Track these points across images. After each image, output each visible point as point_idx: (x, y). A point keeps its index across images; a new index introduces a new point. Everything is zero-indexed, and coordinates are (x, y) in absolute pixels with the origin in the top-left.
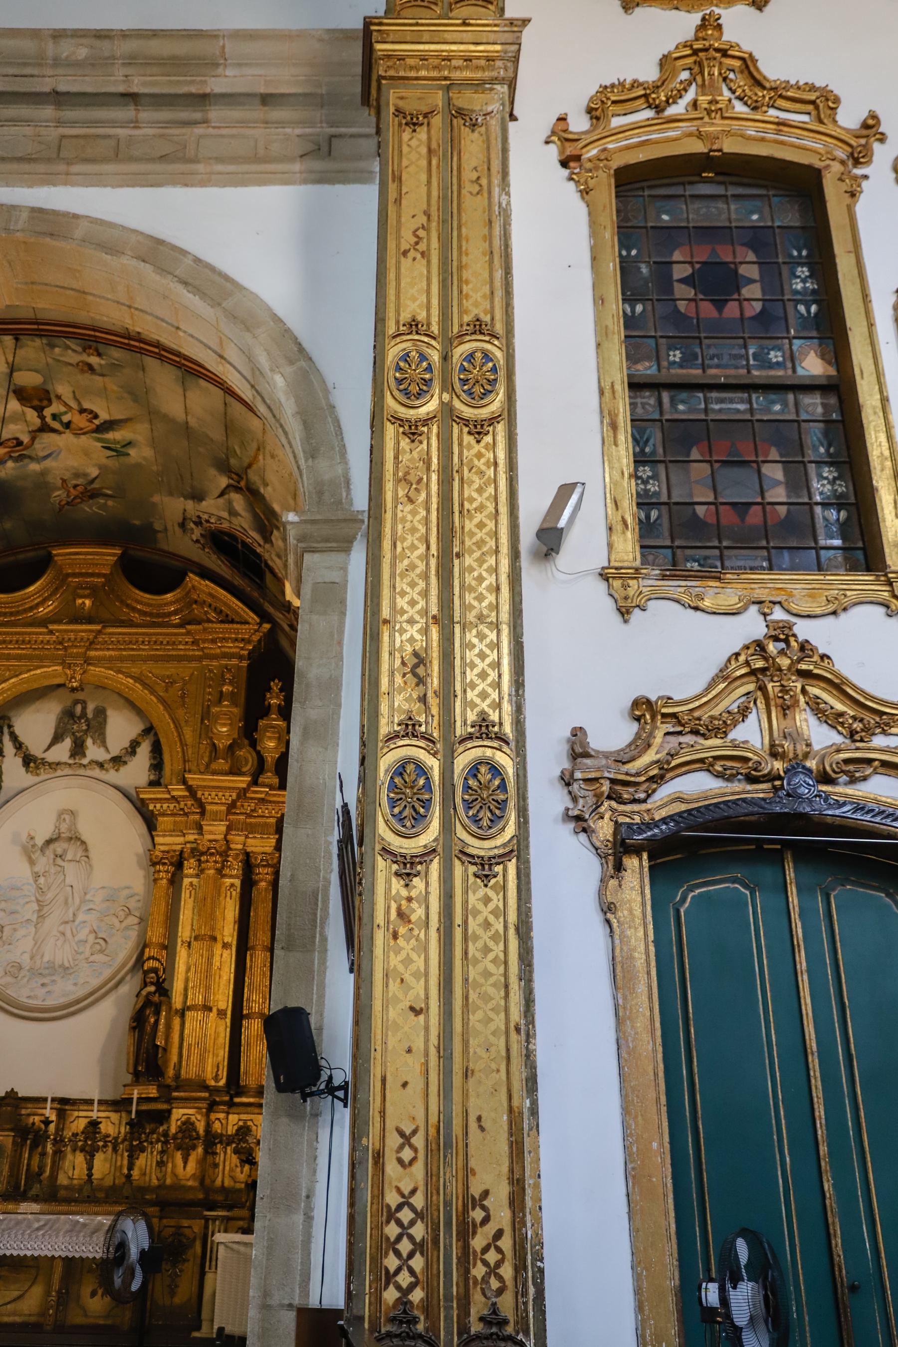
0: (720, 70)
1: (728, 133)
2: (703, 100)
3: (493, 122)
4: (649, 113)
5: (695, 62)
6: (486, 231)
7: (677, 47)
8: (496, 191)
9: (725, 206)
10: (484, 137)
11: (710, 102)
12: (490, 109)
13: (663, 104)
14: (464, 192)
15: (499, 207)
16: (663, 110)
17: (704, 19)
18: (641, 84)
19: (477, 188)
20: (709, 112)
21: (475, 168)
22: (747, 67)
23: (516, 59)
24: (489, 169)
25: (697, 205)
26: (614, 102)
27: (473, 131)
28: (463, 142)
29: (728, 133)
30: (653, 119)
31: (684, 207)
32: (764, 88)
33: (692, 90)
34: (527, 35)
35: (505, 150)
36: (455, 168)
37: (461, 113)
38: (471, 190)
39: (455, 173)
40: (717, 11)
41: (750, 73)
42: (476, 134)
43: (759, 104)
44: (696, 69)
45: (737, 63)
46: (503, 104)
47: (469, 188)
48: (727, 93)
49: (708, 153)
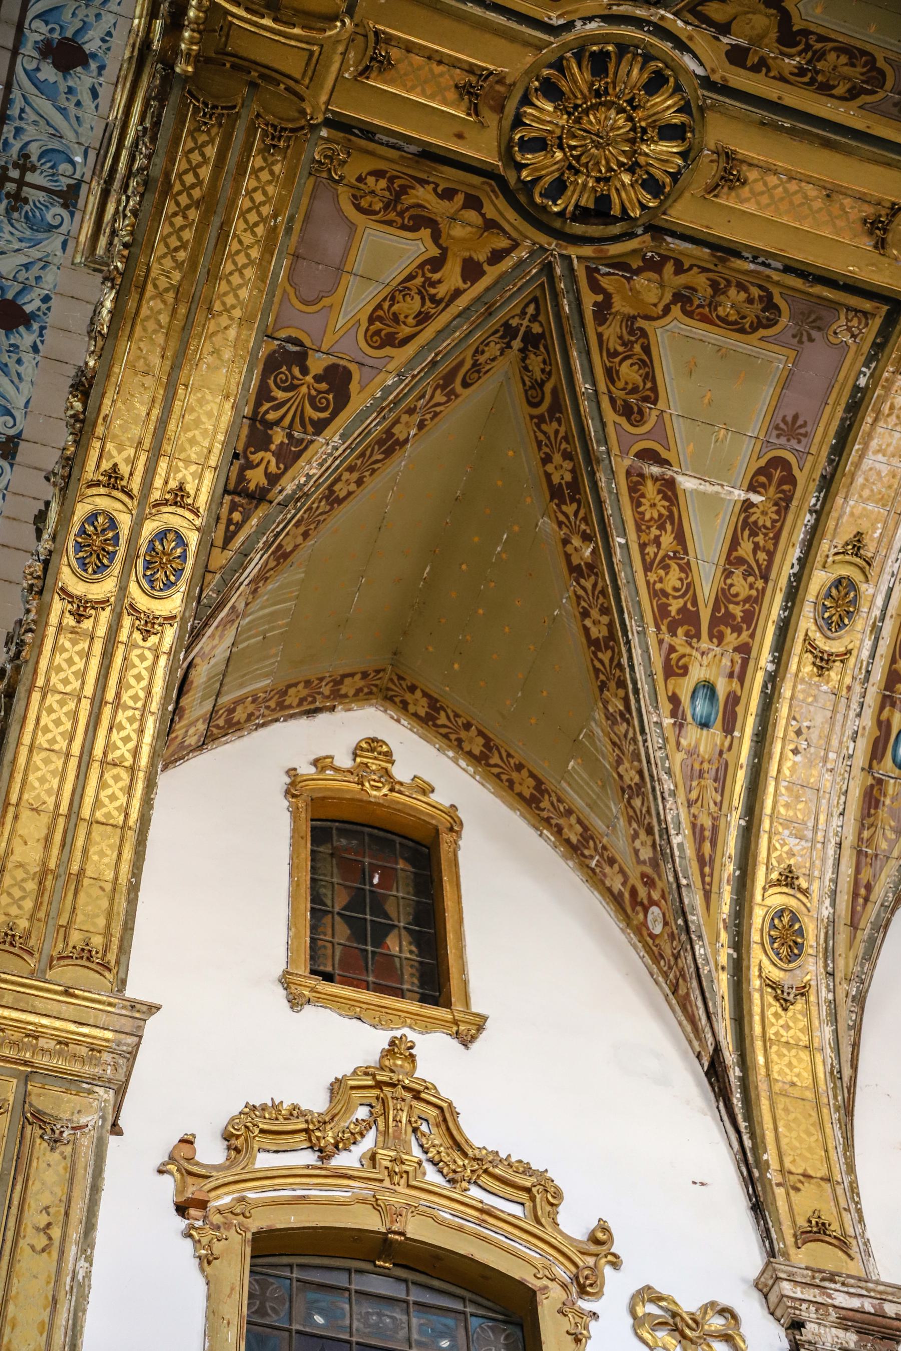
0: (409, 1116)
1: (415, 1210)
2: (385, 1155)
3: (85, 1141)
4: (309, 1158)
5: (377, 1098)
6: (45, 1315)
7: (355, 1072)
8: (72, 1250)
9: (404, 1318)
10: (69, 1159)
11: (393, 1160)
12: (83, 1121)
13: (330, 1148)
14: (22, 1243)
15: (73, 1279)
16: (329, 1157)
17: (392, 1043)
18: (302, 1114)
19: (44, 1241)
20: (391, 1174)
21: (46, 1208)
22: (445, 1120)
23: (132, 1055)
24: (67, 1214)
25: (367, 1307)
26: (262, 1131)
27: (53, 1149)
28: (34, 1164)
29: (415, 1210)
30: (315, 1168)
31: (347, 1307)
32: (465, 1155)
33: (371, 1135)
34: (152, 1026)
35: (96, 1189)
36: (16, 1202)
37: (39, 1118)
38: (34, 1242)
39: (14, 1210)
40: (412, 1035)
41: (448, 1129)
42: (56, 1155)
43: (457, 1177)
44: (378, 1108)
45: (433, 1112)
46: (103, 1118)
47: (32, 1238)
48: (417, 1152)
49: (386, 1234)
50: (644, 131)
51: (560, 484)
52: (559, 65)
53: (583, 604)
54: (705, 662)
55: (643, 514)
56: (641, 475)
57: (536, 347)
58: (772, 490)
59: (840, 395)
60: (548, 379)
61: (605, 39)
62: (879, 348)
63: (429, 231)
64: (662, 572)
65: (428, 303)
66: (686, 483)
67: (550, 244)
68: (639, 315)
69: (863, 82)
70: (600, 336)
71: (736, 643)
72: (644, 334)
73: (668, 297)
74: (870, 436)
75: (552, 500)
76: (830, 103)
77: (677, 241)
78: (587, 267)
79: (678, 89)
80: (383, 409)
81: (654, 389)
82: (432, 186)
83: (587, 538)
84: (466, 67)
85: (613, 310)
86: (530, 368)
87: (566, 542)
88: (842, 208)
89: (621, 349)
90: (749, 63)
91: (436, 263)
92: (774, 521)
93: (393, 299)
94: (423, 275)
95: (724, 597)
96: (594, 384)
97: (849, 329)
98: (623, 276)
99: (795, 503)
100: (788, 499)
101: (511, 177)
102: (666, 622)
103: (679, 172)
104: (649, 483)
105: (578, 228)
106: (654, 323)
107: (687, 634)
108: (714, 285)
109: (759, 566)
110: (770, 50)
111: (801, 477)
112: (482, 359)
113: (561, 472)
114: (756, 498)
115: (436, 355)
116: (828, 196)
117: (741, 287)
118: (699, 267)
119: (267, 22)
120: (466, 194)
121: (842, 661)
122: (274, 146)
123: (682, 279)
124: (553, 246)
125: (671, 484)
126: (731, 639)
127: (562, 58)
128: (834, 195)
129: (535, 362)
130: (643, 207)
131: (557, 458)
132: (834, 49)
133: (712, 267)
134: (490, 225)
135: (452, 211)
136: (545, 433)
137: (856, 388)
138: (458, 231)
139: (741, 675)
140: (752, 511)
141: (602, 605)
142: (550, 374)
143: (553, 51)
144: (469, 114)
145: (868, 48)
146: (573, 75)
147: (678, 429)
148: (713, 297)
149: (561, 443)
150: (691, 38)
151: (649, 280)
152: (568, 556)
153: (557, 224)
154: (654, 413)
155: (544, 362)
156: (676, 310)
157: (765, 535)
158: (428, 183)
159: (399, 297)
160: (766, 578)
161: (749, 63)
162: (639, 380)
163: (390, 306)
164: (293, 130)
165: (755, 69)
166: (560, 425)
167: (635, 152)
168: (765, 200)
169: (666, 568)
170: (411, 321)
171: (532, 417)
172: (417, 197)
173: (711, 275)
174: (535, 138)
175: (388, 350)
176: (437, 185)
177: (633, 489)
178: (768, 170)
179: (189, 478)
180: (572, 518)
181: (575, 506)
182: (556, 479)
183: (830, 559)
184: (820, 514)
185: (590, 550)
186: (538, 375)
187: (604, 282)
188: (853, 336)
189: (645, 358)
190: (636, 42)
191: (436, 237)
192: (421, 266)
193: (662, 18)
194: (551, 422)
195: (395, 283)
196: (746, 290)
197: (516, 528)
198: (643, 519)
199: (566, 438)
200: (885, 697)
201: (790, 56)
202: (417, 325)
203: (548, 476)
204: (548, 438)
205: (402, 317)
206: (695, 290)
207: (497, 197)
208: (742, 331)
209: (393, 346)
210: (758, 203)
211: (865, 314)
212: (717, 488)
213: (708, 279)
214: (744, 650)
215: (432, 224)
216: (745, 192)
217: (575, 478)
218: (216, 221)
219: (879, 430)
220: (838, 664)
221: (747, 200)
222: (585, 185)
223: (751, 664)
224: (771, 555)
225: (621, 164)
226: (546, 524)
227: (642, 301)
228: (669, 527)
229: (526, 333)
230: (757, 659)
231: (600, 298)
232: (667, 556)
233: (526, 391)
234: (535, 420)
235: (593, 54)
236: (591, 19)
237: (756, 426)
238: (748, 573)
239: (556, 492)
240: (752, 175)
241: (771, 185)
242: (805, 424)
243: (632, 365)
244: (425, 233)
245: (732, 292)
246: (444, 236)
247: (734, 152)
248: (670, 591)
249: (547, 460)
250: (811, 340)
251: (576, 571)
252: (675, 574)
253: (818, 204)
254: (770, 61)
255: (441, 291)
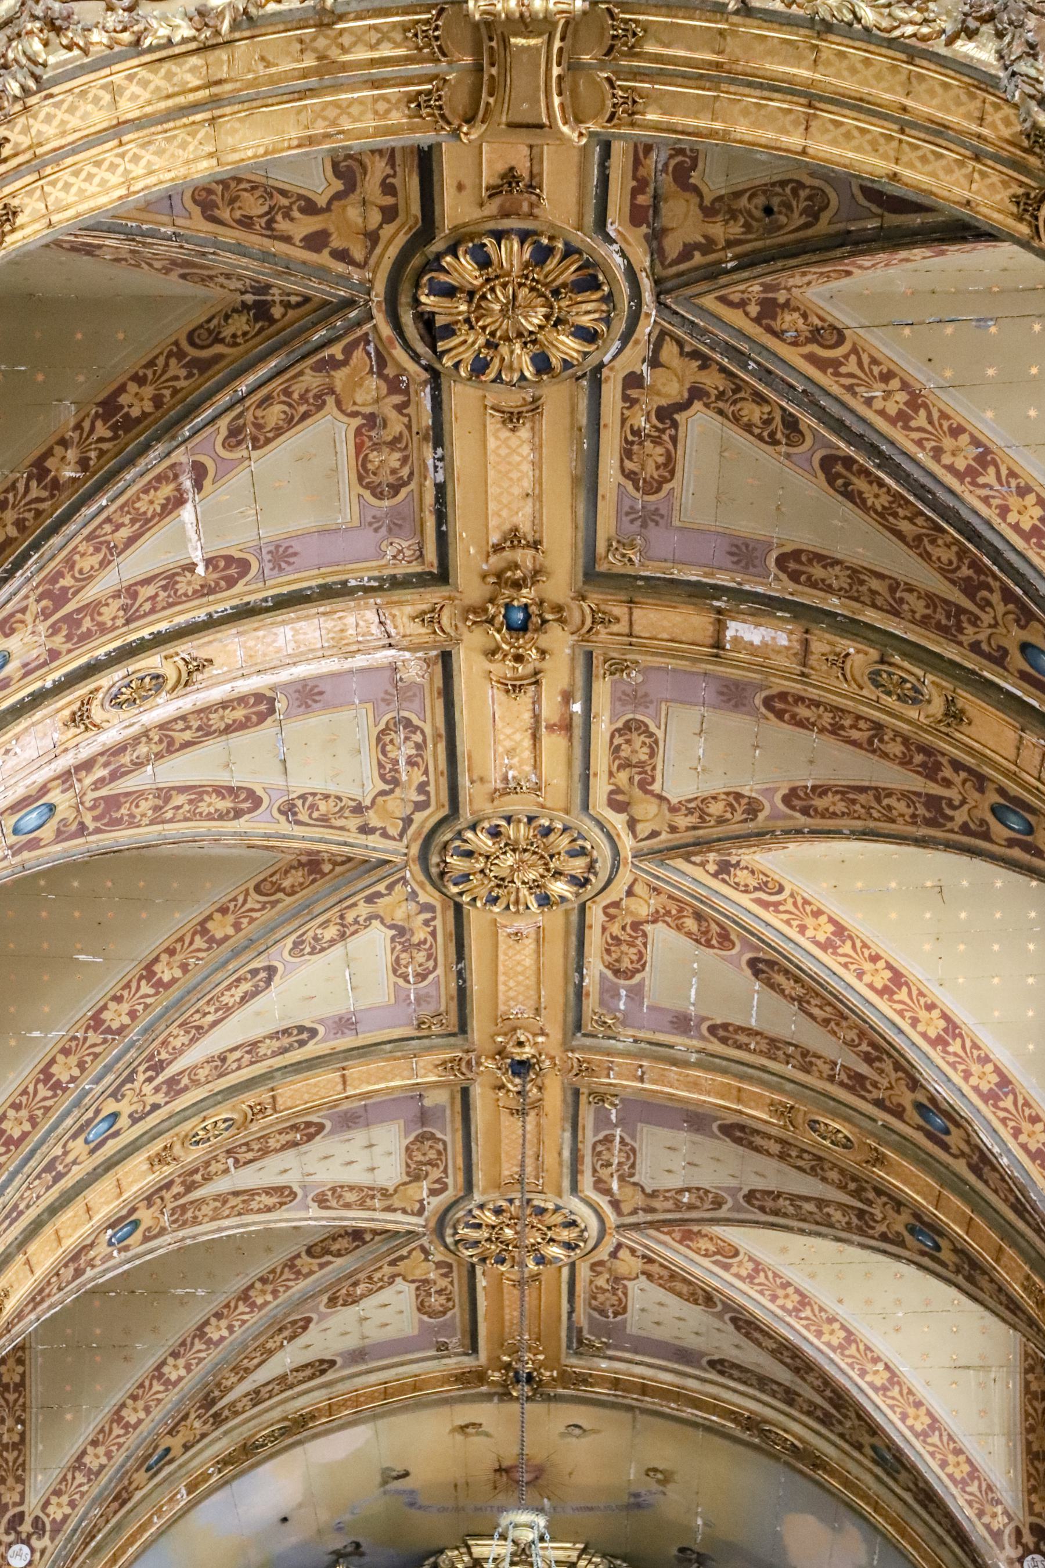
50: (534, 342)
51: (122, 407)
52: (570, 251)
53: (11, 496)
54: (26, 640)
55: (139, 499)
56: (176, 476)
57: (257, 319)
58: (215, 576)
59: (332, 573)
60: (228, 345)
61: (611, 280)
62: (397, 583)
63: (341, 187)
64: (91, 550)
65: (263, 221)
66: (187, 513)
67: (377, 296)
68: (337, 396)
69: (645, 480)
70: (301, 373)
71: (55, 646)
72: (320, 408)
73: (367, 410)
74: (307, 618)
75: (98, 404)
76: (615, 462)
77: (429, 397)
78: (367, 334)
79: (586, 354)
80: (133, 240)
81: (268, 441)
82: (391, 172)
83: (83, 464)
84: (535, 170)
85: (333, 373)
86: (230, 321)
87: (64, 443)
88: (519, 509)
89: (296, 396)
90: (628, 392)
91: (310, 208)
92: (186, 595)
93: (253, 188)
94: (292, 204)
95: (93, 608)
96: (250, 393)
97: (400, 551)
98: (372, 367)
99: (211, 598)
100: (212, 591)
101: (438, 245)
102: (47, 586)
103: (502, 381)
104: (172, 486)
105: (407, 318)
106: (336, 411)
107: (43, 610)
108: (397, 439)
109: (137, 610)
110: (649, 403)
111: (239, 587)
112: (222, 280)
113: (136, 402)
114: (200, 570)
115: (214, 253)
116: (528, 495)
117: (404, 460)
118: (410, 421)
119: (556, 71)
120: (396, 205)
121: (87, 728)
122: (419, 105)
123: (392, 415)
124: (376, 299)
125: (179, 501)
126: (59, 640)
127: (579, 252)
128: (530, 500)
129: (240, 324)
130: (456, 366)
131: (148, 391)
132: (668, 451)
133: (414, 430)
134: (372, 238)
135: (372, 199)
136: (167, 365)
137: (345, 583)
138: (353, 213)
139: (28, 671)
140: (187, 573)
141: (25, 519)
142: (235, 344)
143: (583, 241)
144: (487, 189)
145: (678, 474)
146: (567, 268)
147: (239, 479)
148: (385, 443)
149: (167, 388)
150: (637, 342)
151: (377, 388)
152: (49, 453)
153: (404, 299)
154: (245, 453)
155: (245, 334)
156: (358, 421)
157: (169, 596)
158: (393, 167)
159: (259, 192)
160: (128, 622)
161: (628, 392)
162: (272, 424)
163: (245, 190)
164: (443, 116)
165: (625, 398)
166: (186, 378)
167: (508, 339)
168: (503, 451)
169: (97, 550)
170: (238, 214)
171: (176, 343)
172: (373, 163)
173: (406, 433)
174: (488, 256)
175: (196, 211)
176: (394, 176)
177: (159, 479)
178: (537, 447)
179: (27, 211)
180: (95, 437)
181: (109, 434)
182: (123, 399)
183: (176, 659)
184: (211, 624)
185: (73, 474)
186: (227, 333)
187: (358, 354)
188: (394, 557)
189: (296, 419)
190: (618, 306)
191: (337, 196)
192: (300, 197)
193: (648, 315)
194: (183, 366)
195: (271, 182)
196: (402, 466)
197: (40, 377)
198: (134, 502)
199: (175, 392)
200: (69, 772)
201: (648, 420)
202: (234, 220)
203: (122, 389)
204: (164, 372)
205: (237, 204)
206: (385, 426)
207: (406, 233)
208: (360, 478)
209: (203, 213)
210: (498, 447)
211: (421, 555)
212: (195, 537)
213: (401, 433)
214: (54, 655)
215: (351, 186)
216: (505, 434)
217: (138, 421)
218: (313, 81)
219: (316, 621)
220: (82, 727)
221: (497, 438)
222: (460, 313)
223: (44, 670)
224: (153, 611)
225: (493, 334)
226: (67, 414)
227: (354, 391)
228: (137, 526)
229: (265, 302)
230: (51, 671)
231: (340, 357)
232: (109, 543)
233: (201, 326)
234: (175, 349)
235: (595, 277)
236: (624, 255)
237: (270, 532)
238: (125, 608)
239: (109, 407)
240: (524, 433)
241: (520, 450)
242: (289, 563)
243: (284, 412)
244: (338, 185)
245: (397, 455)
246: (343, 202)
247: (541, 414)
248: (77, 568)
249: (140, 380)
250: (376, 530)
251: (39, 470)
252: (95, 560)
253: (516, 491)
254: (637, 407)
255: (282, 225)
